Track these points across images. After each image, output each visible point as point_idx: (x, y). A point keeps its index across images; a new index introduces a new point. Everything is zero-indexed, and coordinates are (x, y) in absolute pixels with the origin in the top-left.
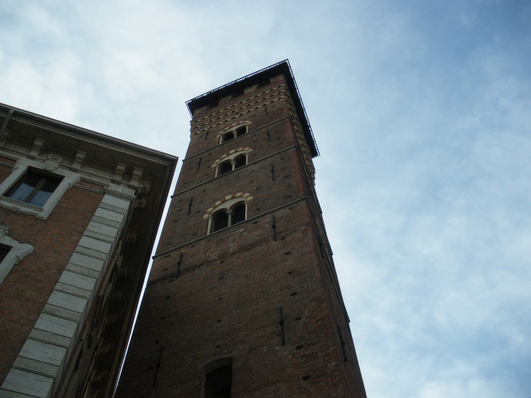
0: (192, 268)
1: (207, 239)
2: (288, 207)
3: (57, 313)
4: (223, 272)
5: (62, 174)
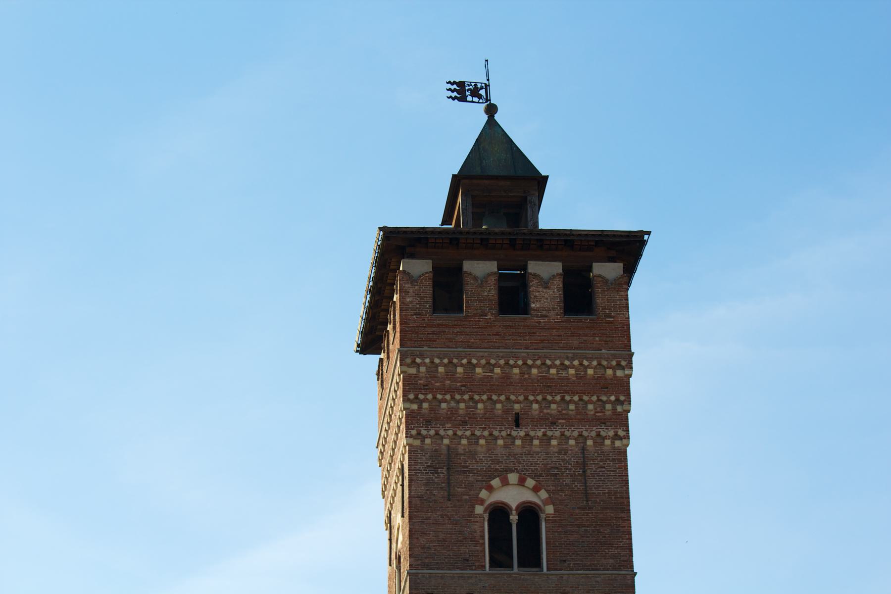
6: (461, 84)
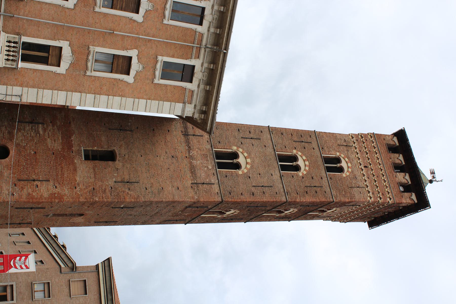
0: (188, 142)
1: (211, 149)
2: (219, 192)
3: (96, 100)
4: (177, 157)
5: (193, 82)
6: (434, 173)
